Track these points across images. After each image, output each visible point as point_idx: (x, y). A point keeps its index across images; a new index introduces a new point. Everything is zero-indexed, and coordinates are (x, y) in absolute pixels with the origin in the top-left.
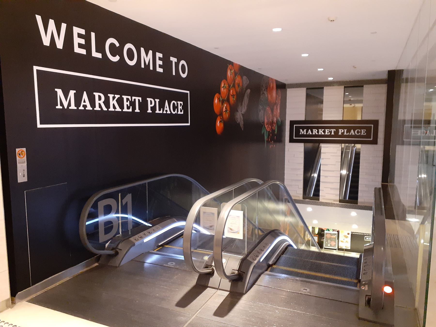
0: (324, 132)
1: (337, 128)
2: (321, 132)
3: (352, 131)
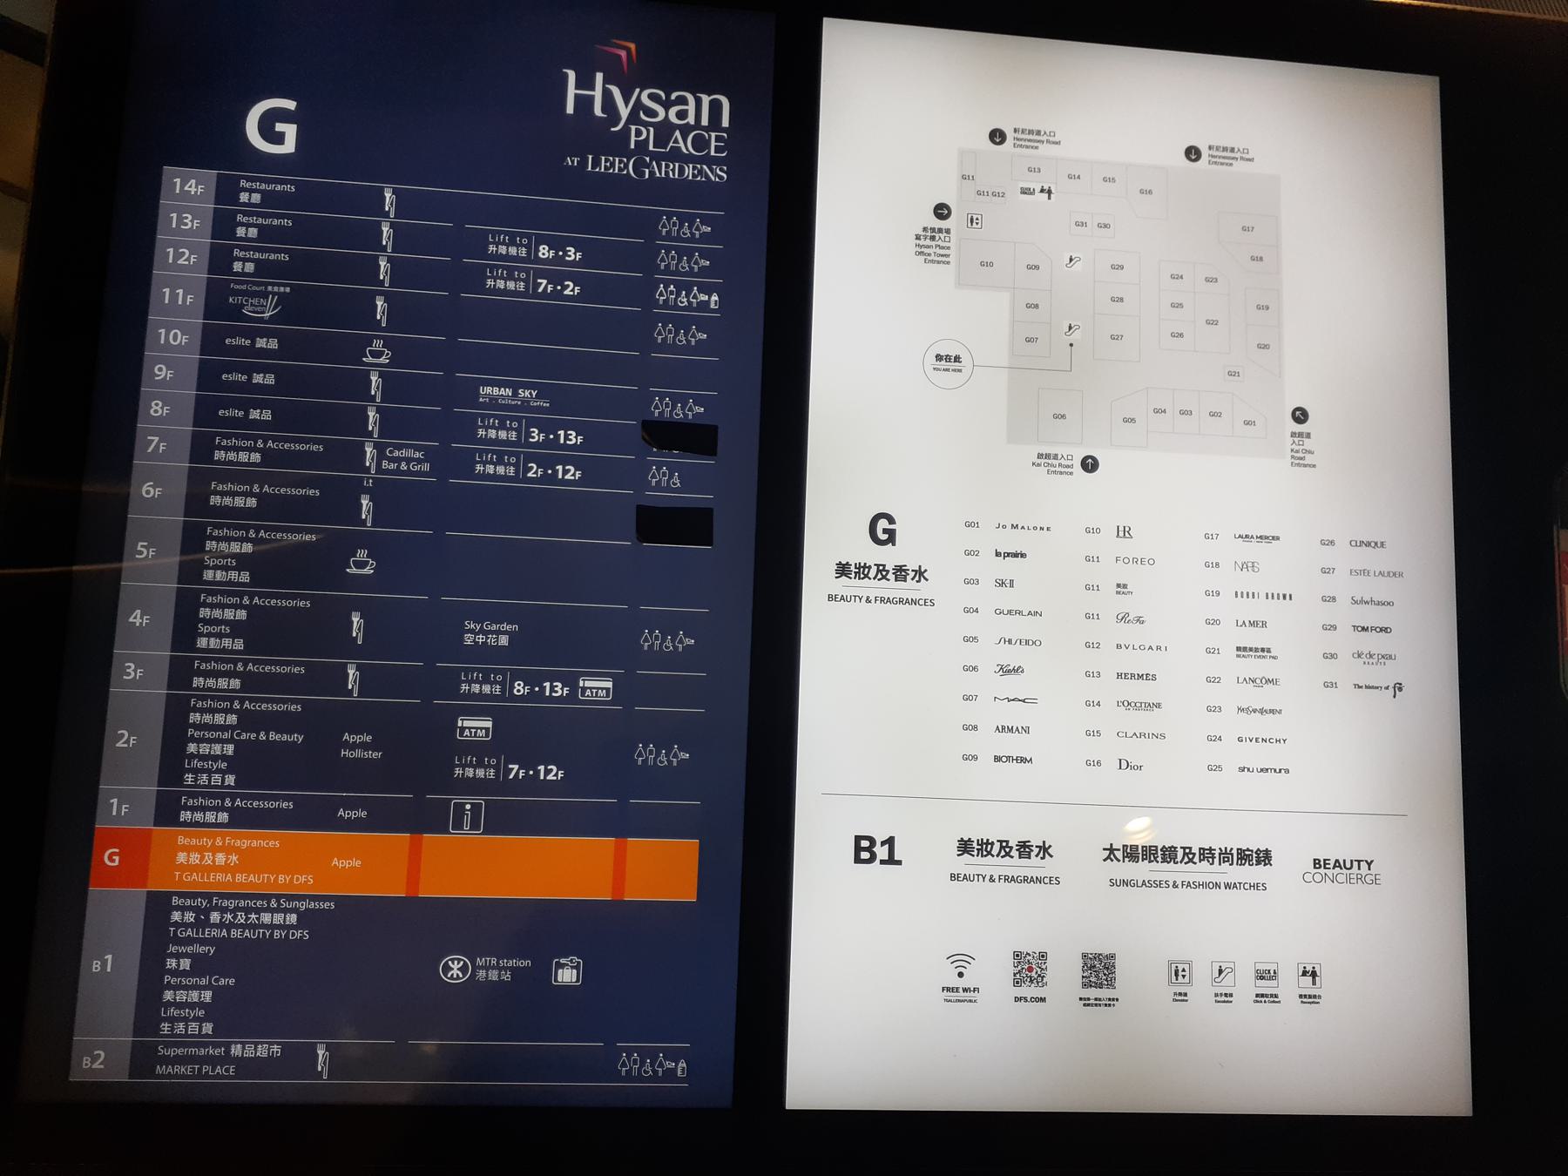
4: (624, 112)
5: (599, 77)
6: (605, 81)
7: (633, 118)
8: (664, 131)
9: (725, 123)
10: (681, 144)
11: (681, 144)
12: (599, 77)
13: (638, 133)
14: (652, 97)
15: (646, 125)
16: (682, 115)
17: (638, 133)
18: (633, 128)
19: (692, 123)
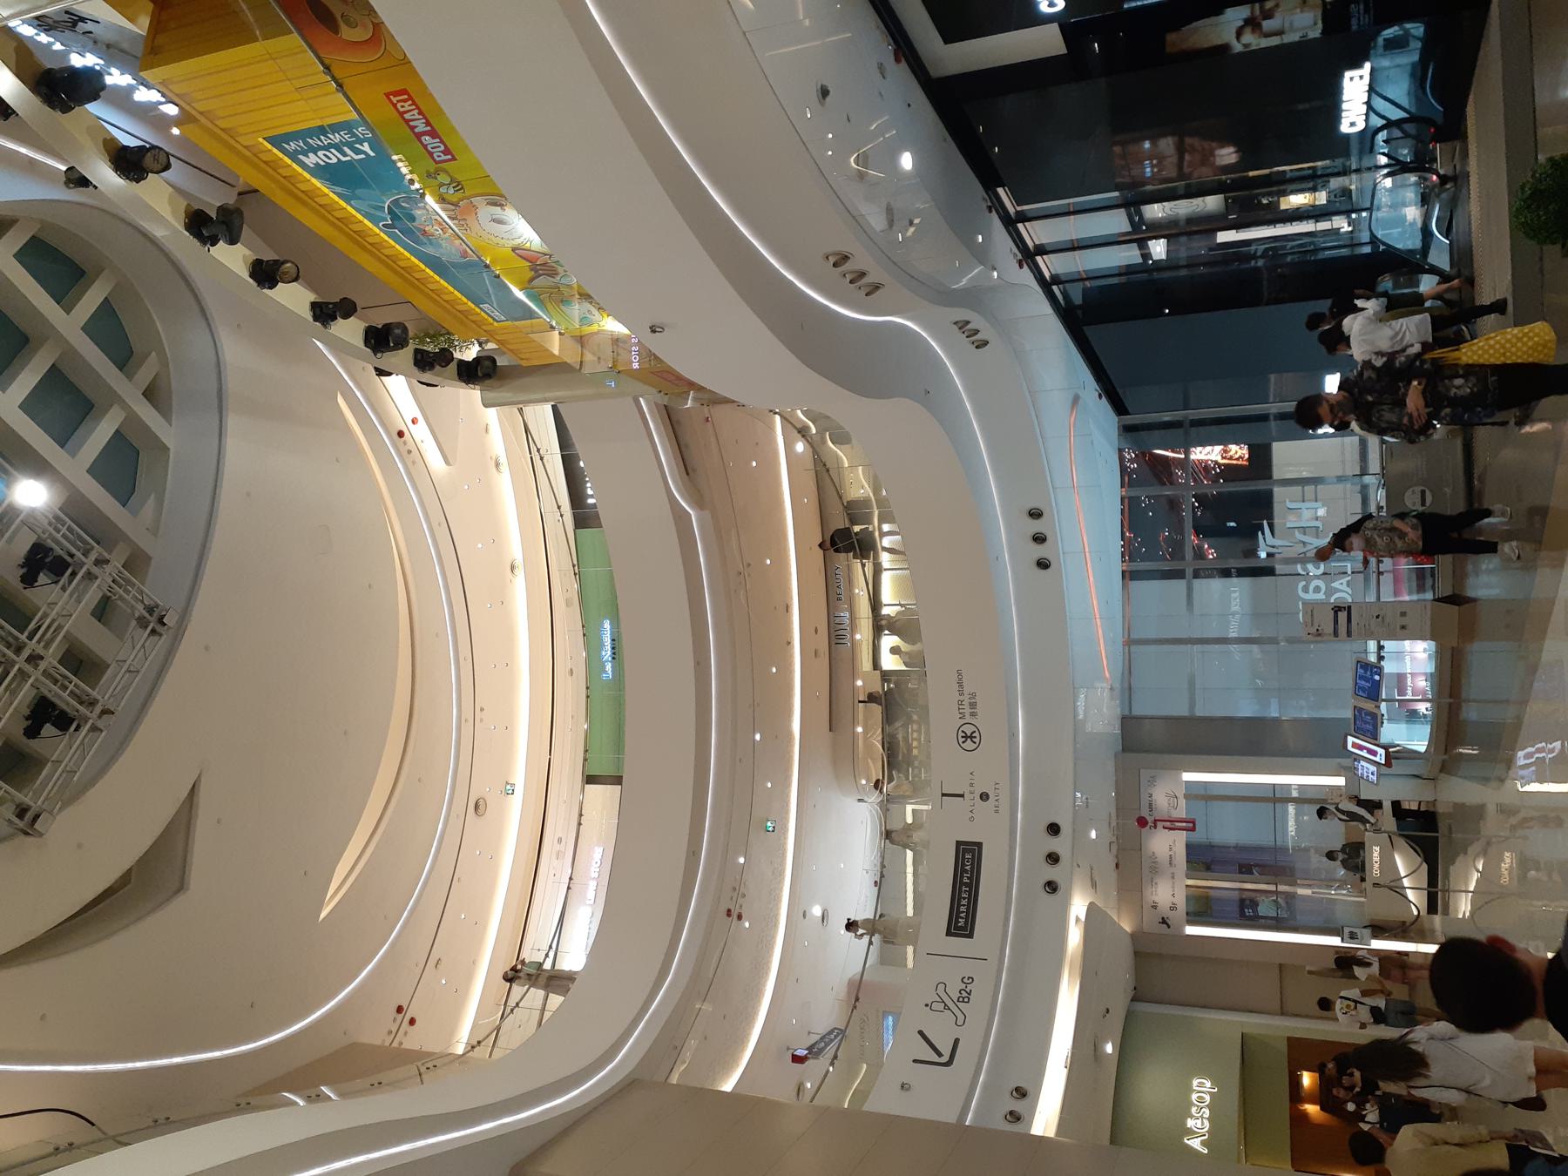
0: (964, 898)
1: (962, 884)
2: (964, 902)
3: (966, 868)
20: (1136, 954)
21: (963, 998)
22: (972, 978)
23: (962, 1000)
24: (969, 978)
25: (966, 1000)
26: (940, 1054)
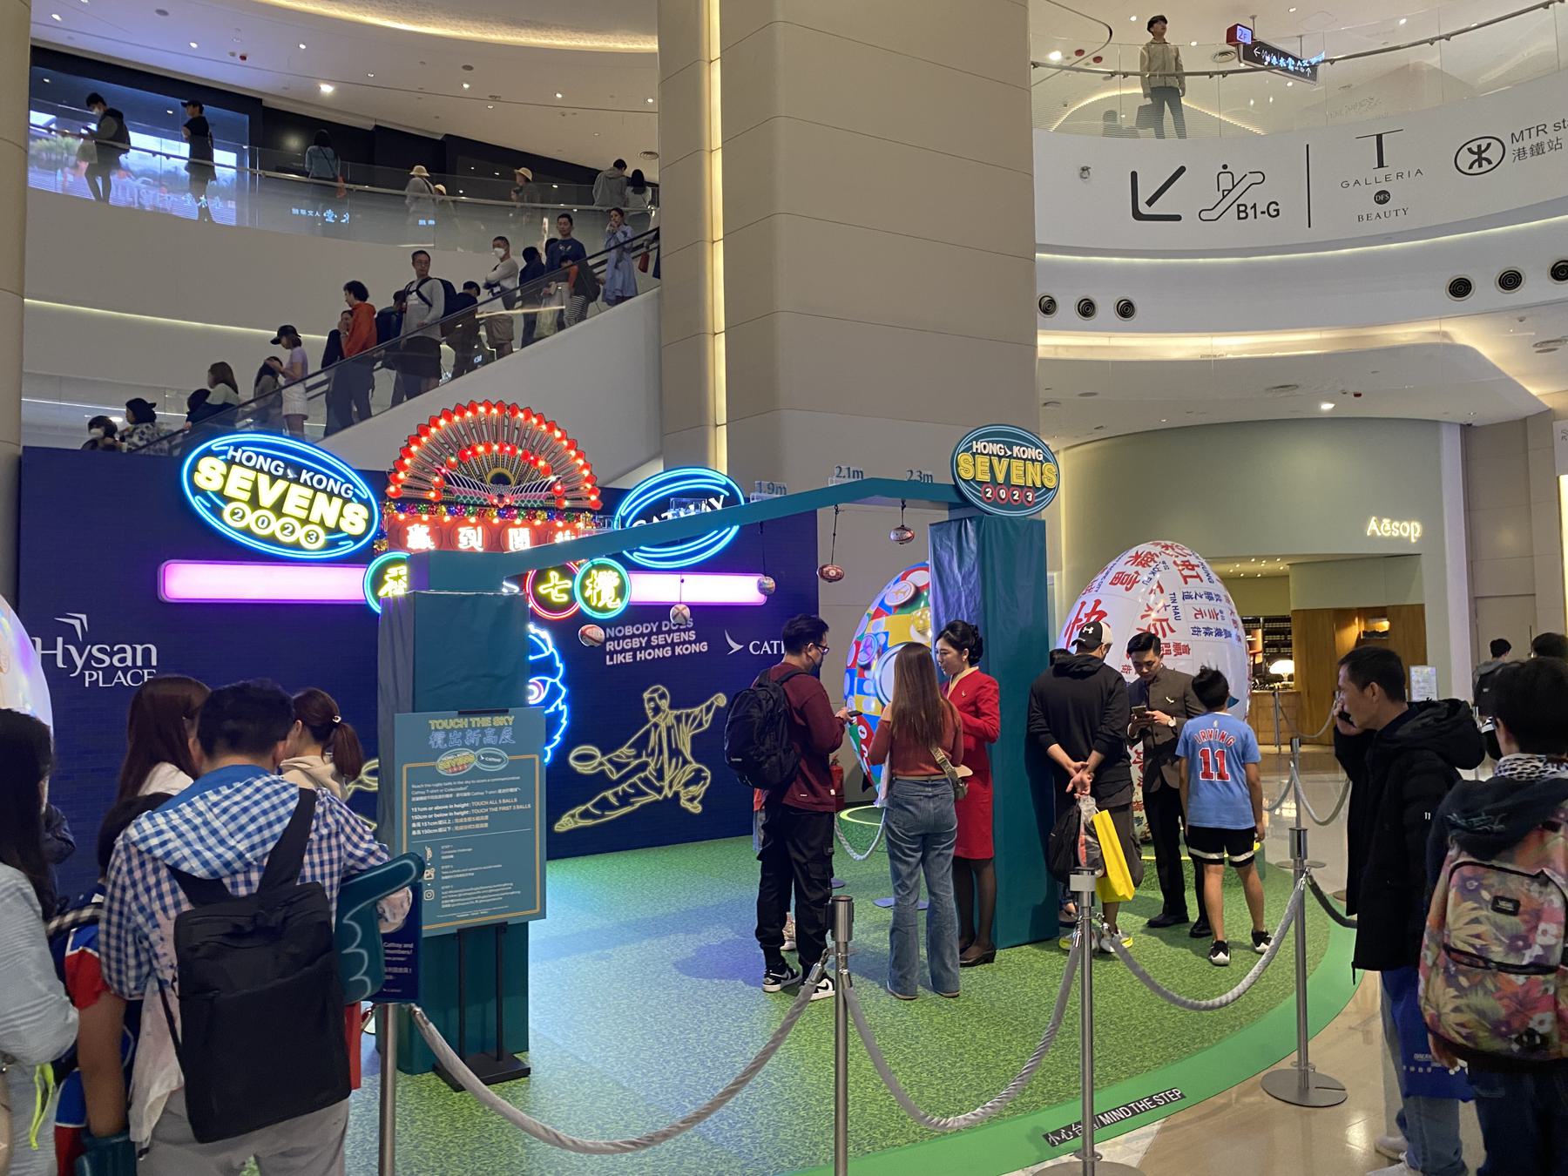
4: (79, 663)
5: (60, 640)
6: (64, 643)
7: (87, 666)
8: (110, 672)
9: (154, 663)
10: (123, 680)
11: (123, 680)
12: (60, 640)
13: (91, 676)
14: (100, 650)
15: (96, 669)
16: (122, 660)
17: (91, 676)
18: (87, 673)
19: (130, 664)
20: (1525, 420)
21: (1244, 211)
22: (1278, 214)
23: (1242, 213)
24: (1278, 210)
25: (1242, 215)
26: (1150, 202)
